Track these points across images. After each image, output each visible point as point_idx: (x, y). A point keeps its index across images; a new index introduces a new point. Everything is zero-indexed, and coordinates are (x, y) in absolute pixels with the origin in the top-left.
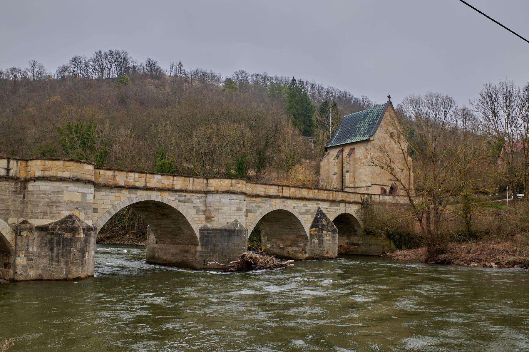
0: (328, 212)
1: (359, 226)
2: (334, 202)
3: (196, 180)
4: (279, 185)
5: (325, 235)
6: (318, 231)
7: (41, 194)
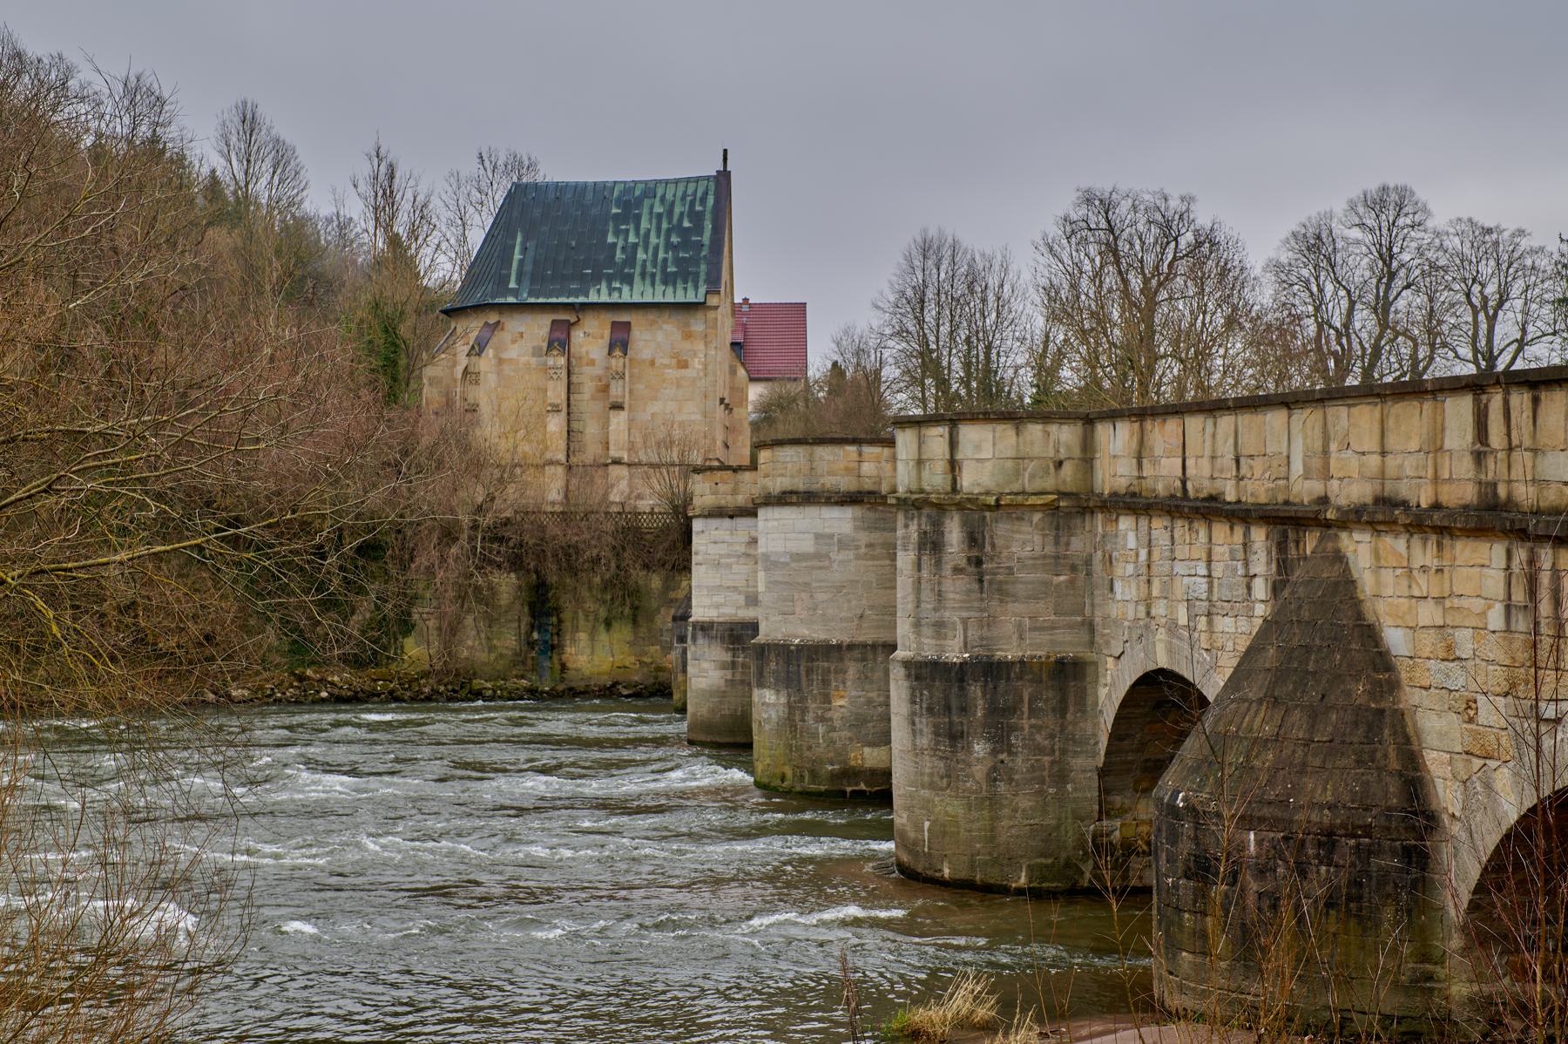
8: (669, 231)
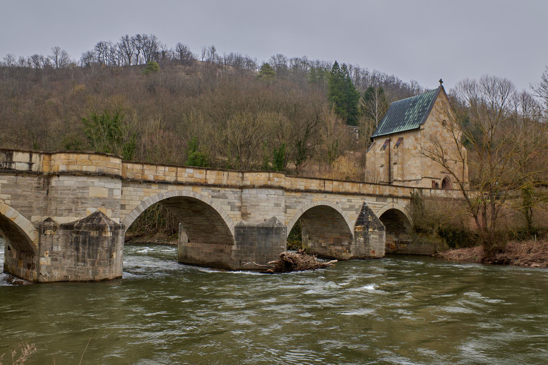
0: (374, 208)
1: (408, 222)
2: (380, 197)
3: (230, 173)
4: (320, 179)
5: (371, 233)
6: (364, 229)
7: (65, 190)
8: (421, 107)
